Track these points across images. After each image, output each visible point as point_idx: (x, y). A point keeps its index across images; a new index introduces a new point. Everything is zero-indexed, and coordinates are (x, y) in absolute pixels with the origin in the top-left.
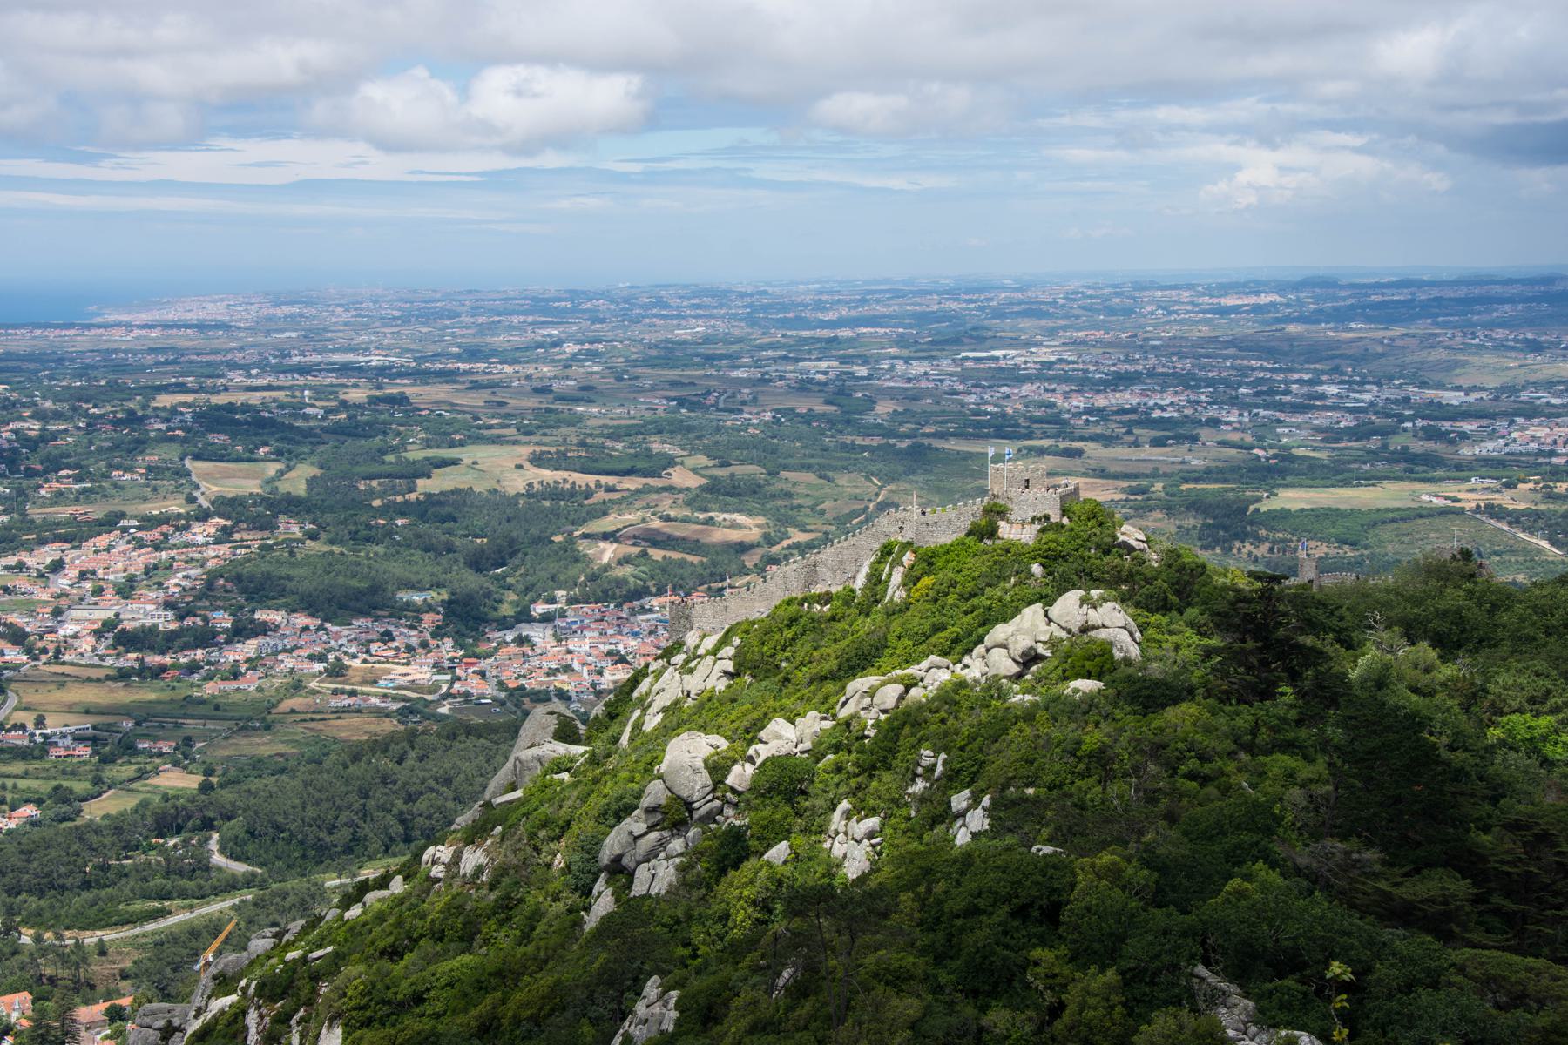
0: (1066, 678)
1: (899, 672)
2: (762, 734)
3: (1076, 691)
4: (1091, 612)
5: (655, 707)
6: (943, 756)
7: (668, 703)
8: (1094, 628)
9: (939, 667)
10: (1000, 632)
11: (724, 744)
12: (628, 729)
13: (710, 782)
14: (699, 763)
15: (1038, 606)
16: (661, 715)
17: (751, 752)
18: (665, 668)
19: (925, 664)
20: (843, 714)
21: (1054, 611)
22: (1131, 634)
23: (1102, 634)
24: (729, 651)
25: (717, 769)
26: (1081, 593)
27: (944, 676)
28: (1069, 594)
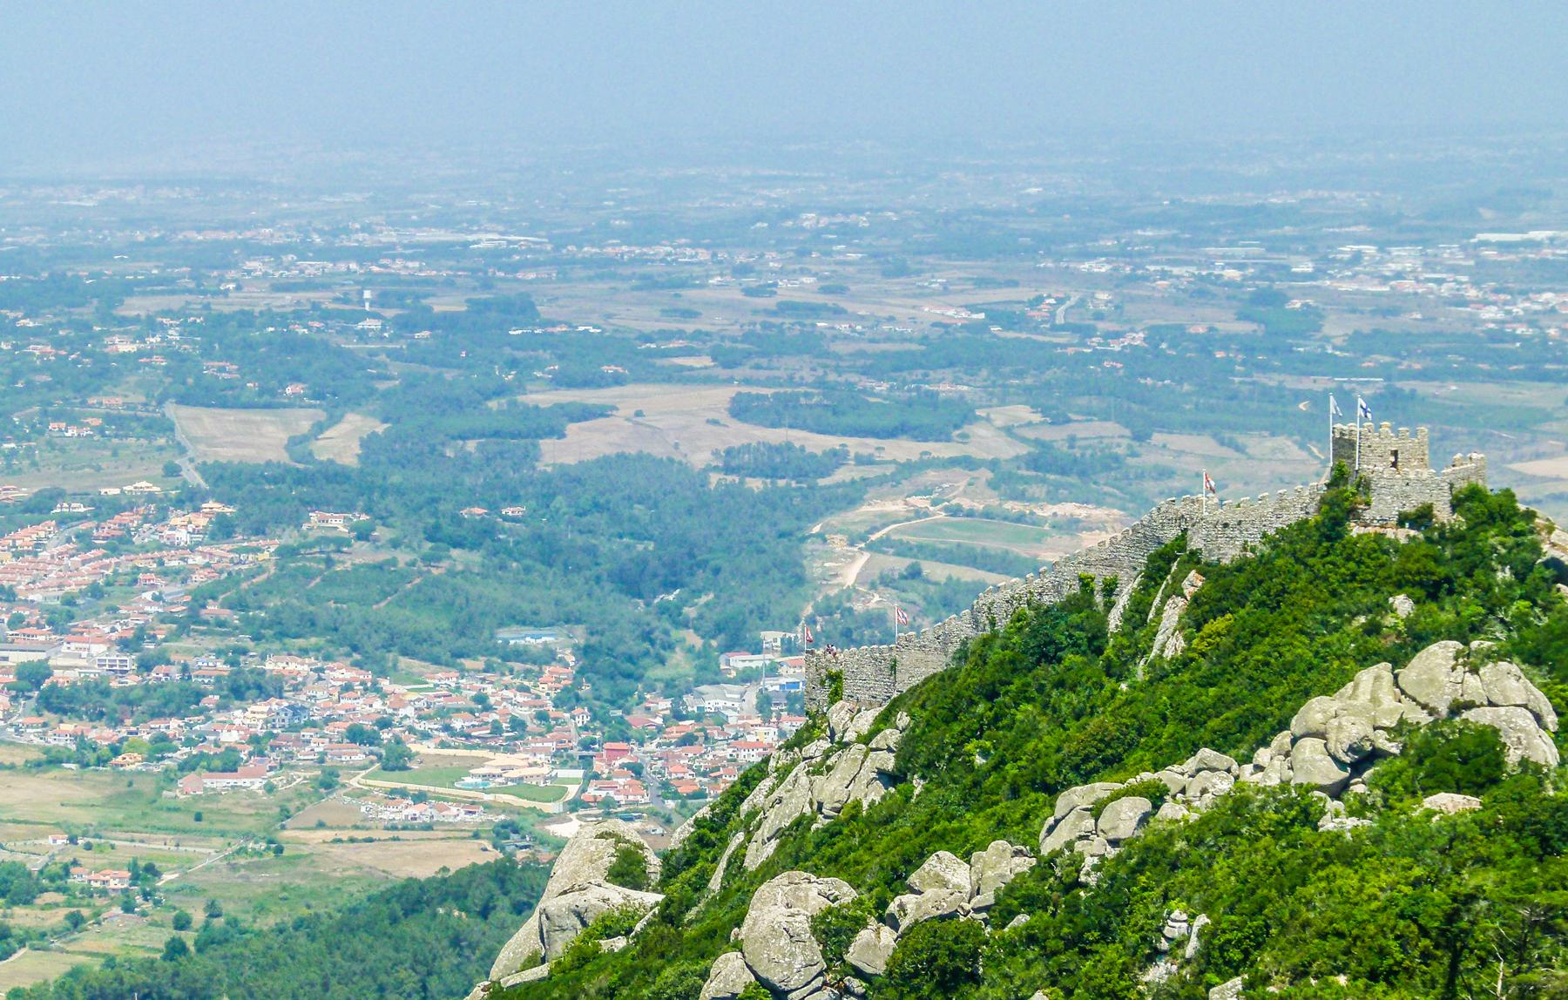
1: (1147, 776)
2: (914, 879)
4: (1471, 680)
5: (765, 831)
6: (1203, 919)
7: (787, 823)
8: (1469, 706)
10: (1316, 710)
11: (847, 894)
12: (723, 864)
13: (818, 957)
14: (802, 924)
15: (1384, 668)
16: (774, 843)
17: (893, 907)
18: (794, 763)
19: (1191, 764)
20: (1049, 845)
21: (1409, 675)
22: (1538, 718)
25: (834, 933)
26: (1454, 645)
27: (1223, 784)
28: (1433, 648)
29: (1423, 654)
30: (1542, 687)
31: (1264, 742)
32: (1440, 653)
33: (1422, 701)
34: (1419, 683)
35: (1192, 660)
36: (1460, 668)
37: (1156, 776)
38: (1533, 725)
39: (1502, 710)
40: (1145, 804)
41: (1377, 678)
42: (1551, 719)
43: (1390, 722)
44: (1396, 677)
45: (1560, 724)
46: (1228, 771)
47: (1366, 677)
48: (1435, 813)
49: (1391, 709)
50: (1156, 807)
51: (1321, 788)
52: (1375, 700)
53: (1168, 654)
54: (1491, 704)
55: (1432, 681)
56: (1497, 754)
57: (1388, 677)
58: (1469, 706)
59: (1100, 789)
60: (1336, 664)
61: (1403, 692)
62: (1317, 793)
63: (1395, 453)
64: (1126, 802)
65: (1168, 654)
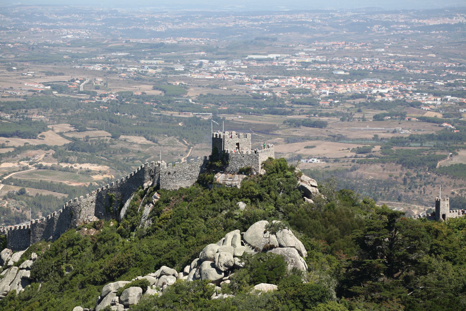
0: (254, 282)
1: (140, 278)
3: (258, 292)
4: (273, 237)
8: (272, 247)
9: (168, 275)
10: (211, 249)
15: (237, 232)
19: (158, 273)
21: (248, 235)
22: (300, 252)
23: (279, 251)
24: (29, 263)
26: (265, 222)
27: (171, 281)
28: (257, 223)
29: (253, 226)
30: (301, 239)
31: (189, 263)
32: (259, 227)
33: (253, 245)
34: (252, 238)
35: (156, 229)
36: (268, 232)
37: (144, 277)
38: (298, 255)
39: (285, 249)
40: (140, 290)
41: (235, 236)
42: (304, 252)
43: (240, 254)
44: (242, 235)
45: (308, 254)
46: (174, 275)
47: (230, 236)
48: (259, 291)
49: (241, 250)
50: (144, 292)
51: (213, 282)
52: (233, 245)
53: (146, 227)
54: (281, 246)
55: (257, 237)
56: (283, 266)
57: (239, 236)
58: (272, 247)
59: (121, 283)
60: (215, 230)
61: (245, 242)
62: (211, 284)
63: (238, 144)
64: (132, 289)
65: (146, 227)
